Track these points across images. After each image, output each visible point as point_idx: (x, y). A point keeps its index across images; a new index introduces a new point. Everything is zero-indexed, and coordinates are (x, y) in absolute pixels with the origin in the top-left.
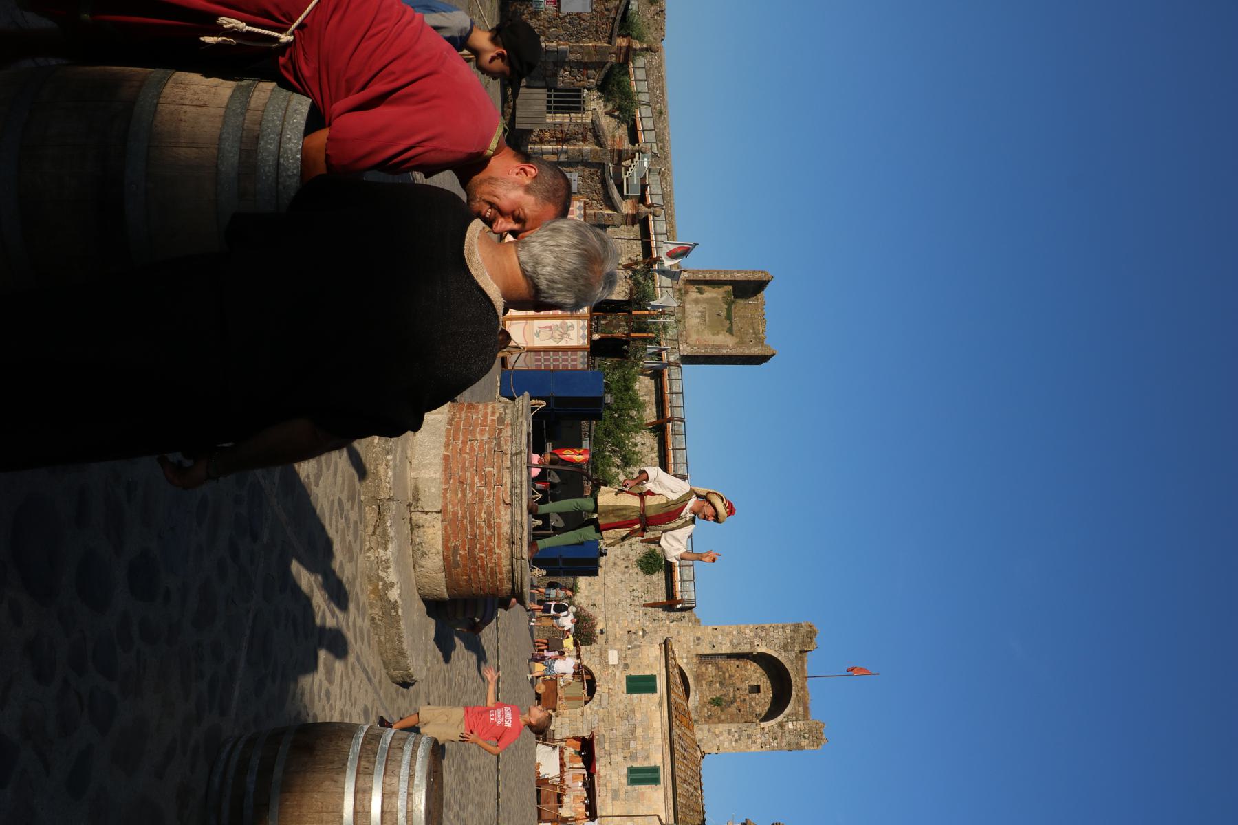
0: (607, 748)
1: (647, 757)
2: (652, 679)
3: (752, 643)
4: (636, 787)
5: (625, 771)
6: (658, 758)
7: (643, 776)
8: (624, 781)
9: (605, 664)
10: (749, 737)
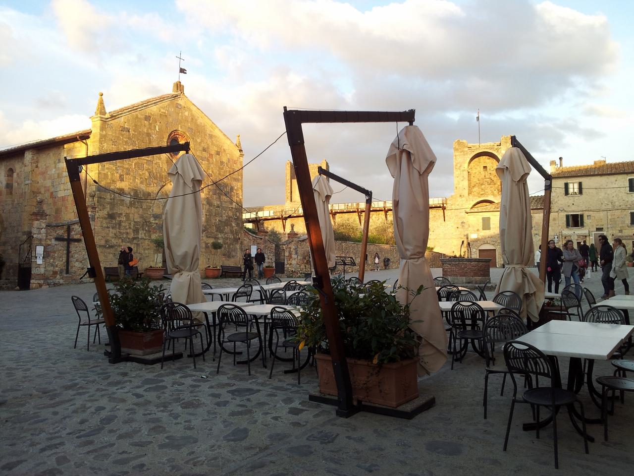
2: (484, 219)
3: (463, 171)
4: (533, 226)
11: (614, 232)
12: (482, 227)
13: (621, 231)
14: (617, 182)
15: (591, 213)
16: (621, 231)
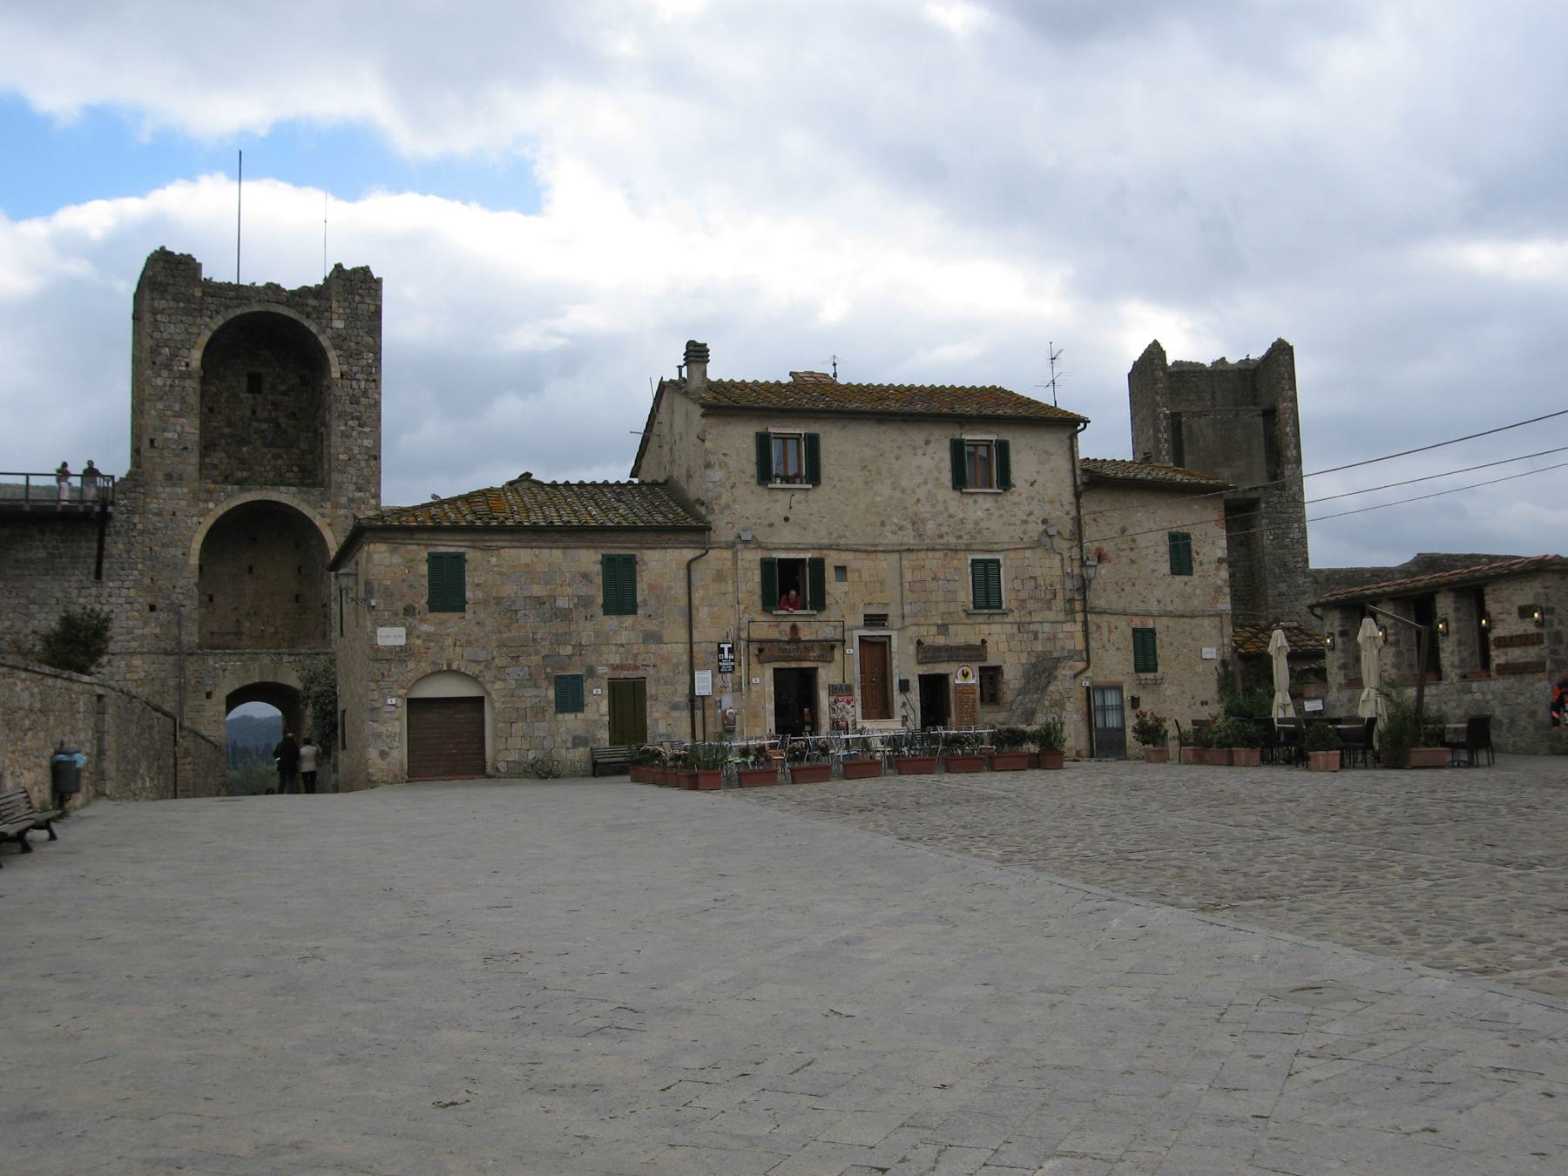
0: (569, 650)
1: (586, 577)
4: (639, 599)
5: (612, 622)
6: (589, 559)
7: (620, 591)
8: (628, 620)
9: (401, 654)
10: (355, 401)
11: (923, 630)
12: (426, 598)
13: (943, 629)
14: (930, 449)
15: (845, 558)
16: (943, 629)
